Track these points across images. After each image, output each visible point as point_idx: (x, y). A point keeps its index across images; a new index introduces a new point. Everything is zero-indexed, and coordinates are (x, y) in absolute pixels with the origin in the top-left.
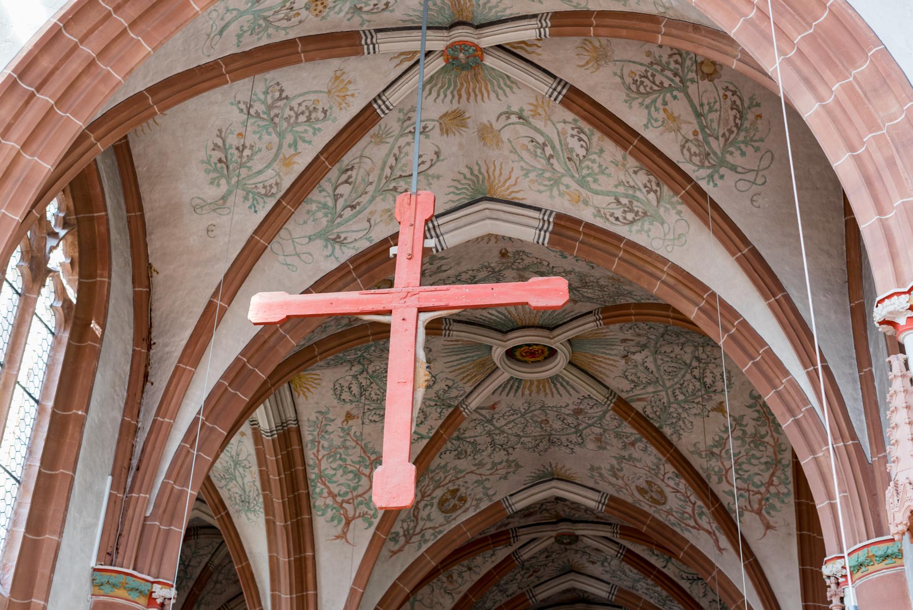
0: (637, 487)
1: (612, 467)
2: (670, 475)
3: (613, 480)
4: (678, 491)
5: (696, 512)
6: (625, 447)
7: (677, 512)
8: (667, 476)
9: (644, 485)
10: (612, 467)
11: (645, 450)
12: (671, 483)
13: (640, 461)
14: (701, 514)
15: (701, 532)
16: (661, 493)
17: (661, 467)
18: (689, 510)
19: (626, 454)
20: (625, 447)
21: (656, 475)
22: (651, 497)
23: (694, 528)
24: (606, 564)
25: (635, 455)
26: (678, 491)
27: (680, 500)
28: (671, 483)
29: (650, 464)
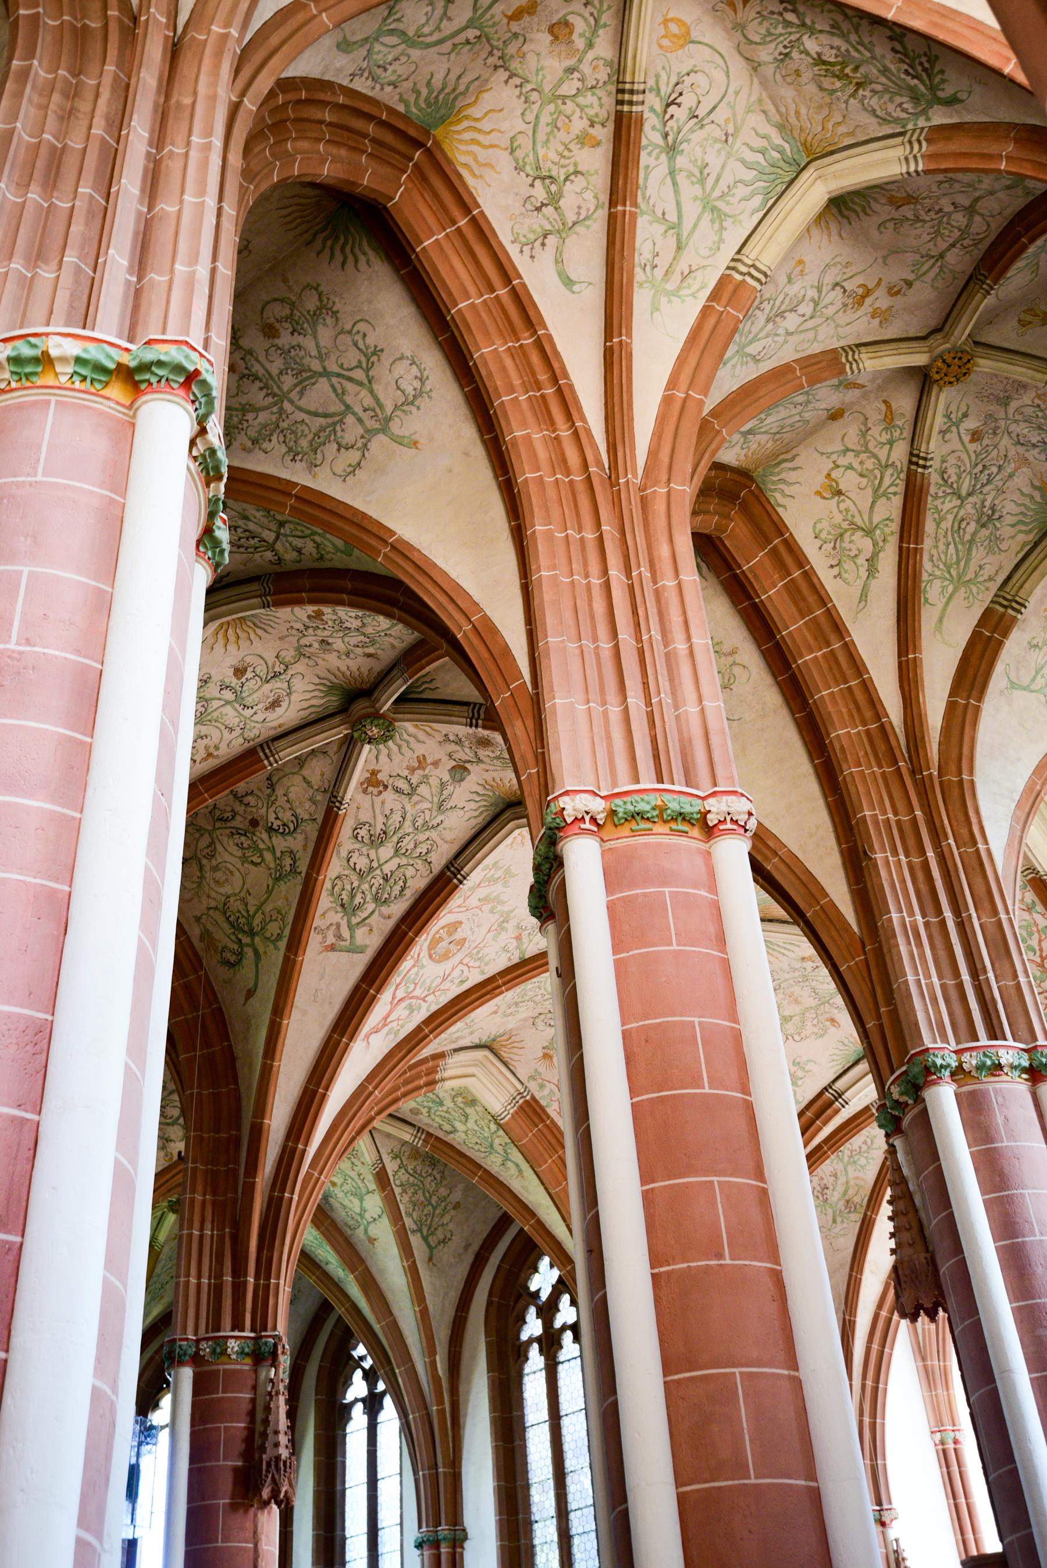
0: (461, 923)
1: (501, 903)
2: (466, 973)
3: (481, 893)
4: (444, 980)
5: (414, 1001)
6: (519, 927)
7: (417, 974)
8: (466, 969)
9: (459, 934)
10: (501, 903)
11: (505, 949)
12: (456, 973)
13: (495, 939)
14: (411, 1009)
15: (389, 1007)
16: (446, 956)
17: (477, 964)
18: (418, 992)
19: (510, 926)
20: (519, 927)
21: (470, 955)
22: (441, 939)
23: (393, 998)
24: (228, 695)
25: (503, 935)
26: (444, 980)
27: (432, 982)
28: (456, 973)
29: (486, 951)
